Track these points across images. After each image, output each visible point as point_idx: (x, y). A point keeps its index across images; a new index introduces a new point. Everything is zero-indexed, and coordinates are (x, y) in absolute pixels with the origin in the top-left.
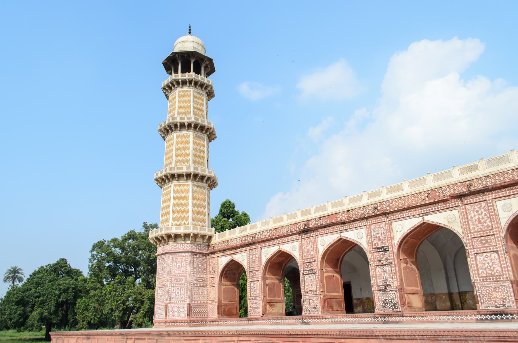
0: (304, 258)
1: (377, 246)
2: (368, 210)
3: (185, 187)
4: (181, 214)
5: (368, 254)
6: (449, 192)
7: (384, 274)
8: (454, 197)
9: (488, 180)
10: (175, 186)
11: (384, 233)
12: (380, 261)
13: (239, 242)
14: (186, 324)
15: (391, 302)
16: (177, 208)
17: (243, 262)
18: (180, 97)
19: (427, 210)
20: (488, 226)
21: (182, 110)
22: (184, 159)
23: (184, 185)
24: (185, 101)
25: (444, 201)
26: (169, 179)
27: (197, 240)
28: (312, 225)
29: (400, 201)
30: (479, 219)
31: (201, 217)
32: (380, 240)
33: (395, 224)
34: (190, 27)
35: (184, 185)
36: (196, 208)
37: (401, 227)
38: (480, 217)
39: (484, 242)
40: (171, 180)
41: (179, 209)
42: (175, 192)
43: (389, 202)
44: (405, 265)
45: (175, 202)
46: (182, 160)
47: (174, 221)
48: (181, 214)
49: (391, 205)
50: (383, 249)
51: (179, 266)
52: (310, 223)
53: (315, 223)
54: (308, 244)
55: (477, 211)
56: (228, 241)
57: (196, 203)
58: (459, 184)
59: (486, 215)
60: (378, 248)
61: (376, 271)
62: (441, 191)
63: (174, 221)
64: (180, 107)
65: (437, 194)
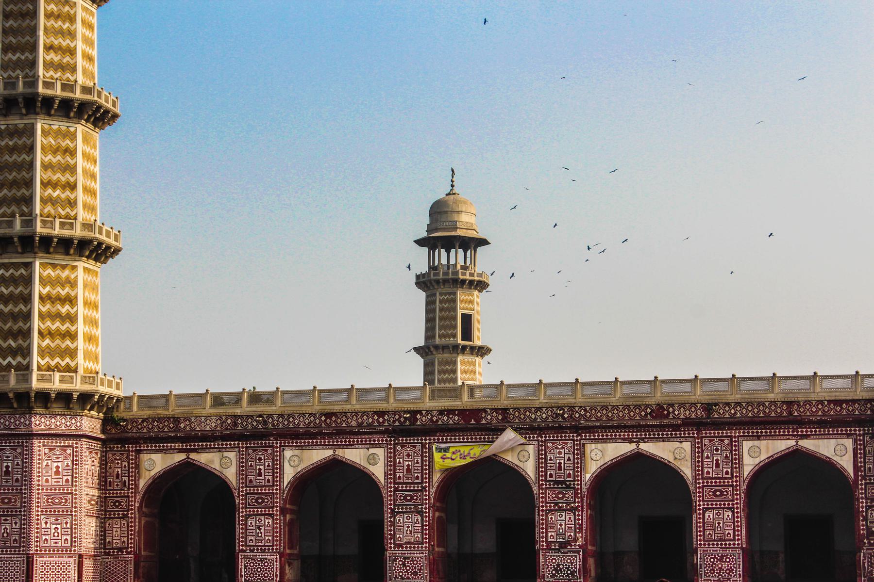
0: (397, 481)
1: (554, 478)
2: (544, 416)
4: (58, 341)
5: (535, 489)
6: (683, 414)
7: (561, 525)
8: (688, 423)
9: (738, 408)
11: (569, 459)
12: (556, 504)
13: (211, 425)
15: (568, 569)
16: (49, 323)
17: (225, 472)
19: (645, 435)
20: (727, 473)
21: (53, 56)
22: (63, 196)
24: (61, 33)
25: (676, 428)
28: (421, 420)
29: (604, 412)
30: (717, 460)
32: (560, 468)
33: (590, 447)
35: (64, 267)
37: (600, 453)
38: (719, 458)
39: (718, 493)
41: (53, 327)
43: (585, 410)
45: (44, 309)
46: (58, 197)
47: (43, 357)
48: (58, 341)
49: (588, 415)
51: (58, 467)
52: (418, 416)
53: (431, 419)
54: (408, 455)
55: (717, 450)
56: (177, 420)
58: (699, 405)
59: (727, 457)
60: (556, 482)
61: (546, 519)
62: (671, 410)
63: (43, 357)
65: (665, 412)
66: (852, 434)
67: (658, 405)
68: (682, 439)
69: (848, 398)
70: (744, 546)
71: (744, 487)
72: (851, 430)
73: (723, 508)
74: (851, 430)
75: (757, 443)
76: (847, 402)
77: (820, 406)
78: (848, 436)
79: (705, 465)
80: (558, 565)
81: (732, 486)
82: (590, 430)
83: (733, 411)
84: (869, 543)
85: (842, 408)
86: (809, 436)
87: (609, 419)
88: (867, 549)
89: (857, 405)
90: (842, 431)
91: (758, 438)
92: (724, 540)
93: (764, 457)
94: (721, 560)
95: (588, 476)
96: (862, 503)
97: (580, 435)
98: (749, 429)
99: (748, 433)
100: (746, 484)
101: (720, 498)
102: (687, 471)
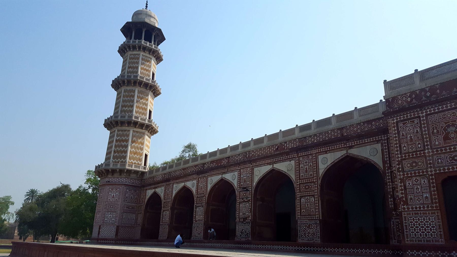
1: (242, 187)
3: (126, 132)
4: (120, 154)
10: (118, 131)
14: (113, 242)
18: (130, 59)
23: (125, 131)
25: (287, 153)
26: (113, 125)
27: (131, 175)
31: (138, 157)
34: (147, 2)
36: (133, 149)
40: (115, 125)
42: (117, 136)
44: (261, 203)
47: (114, 159)
50: (245, 189)
57: (134, 146)
64: (129, 68)
66: (380, 140)
67: (281, 143)
68: (291, 159)
69: (374, 118)
70: (321, 218)
71: (319, 182)
72: (378, 138)
73: (309, 196)
74: (378, 138)
75: (325, 155)
76: (374, 120)
77: (359, 127)
78: (378, 142)
79: (301, 172)
80: (242, 230)
81: (313, 182)
82: (255, 161)
83: (313, 140)
84: (396, 214)
85: (372, 125)
86: (354, 146)
87: (259, 156)
88: (395, 219)
89: (381, 121)
90: (373, 139)
91: (326, 152)
92: (311, 215)
93: (329, 163)
94: (309, 227)
95: (254, 184)
96: (390, 185)
97: (252, 164)
98: (321, 148)
99: (320, 150)
100: (320, 180)
101: (308, 190)
102: (293, 176)
